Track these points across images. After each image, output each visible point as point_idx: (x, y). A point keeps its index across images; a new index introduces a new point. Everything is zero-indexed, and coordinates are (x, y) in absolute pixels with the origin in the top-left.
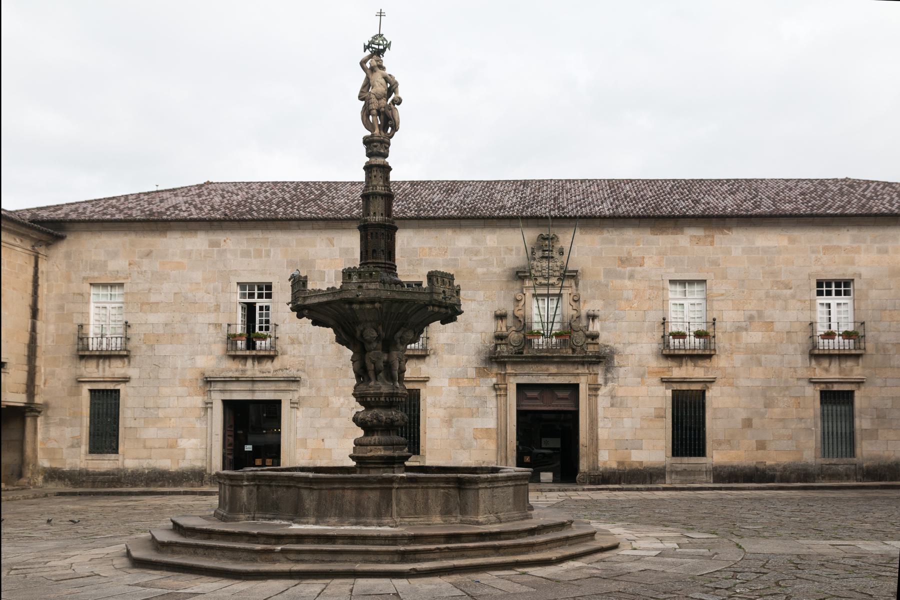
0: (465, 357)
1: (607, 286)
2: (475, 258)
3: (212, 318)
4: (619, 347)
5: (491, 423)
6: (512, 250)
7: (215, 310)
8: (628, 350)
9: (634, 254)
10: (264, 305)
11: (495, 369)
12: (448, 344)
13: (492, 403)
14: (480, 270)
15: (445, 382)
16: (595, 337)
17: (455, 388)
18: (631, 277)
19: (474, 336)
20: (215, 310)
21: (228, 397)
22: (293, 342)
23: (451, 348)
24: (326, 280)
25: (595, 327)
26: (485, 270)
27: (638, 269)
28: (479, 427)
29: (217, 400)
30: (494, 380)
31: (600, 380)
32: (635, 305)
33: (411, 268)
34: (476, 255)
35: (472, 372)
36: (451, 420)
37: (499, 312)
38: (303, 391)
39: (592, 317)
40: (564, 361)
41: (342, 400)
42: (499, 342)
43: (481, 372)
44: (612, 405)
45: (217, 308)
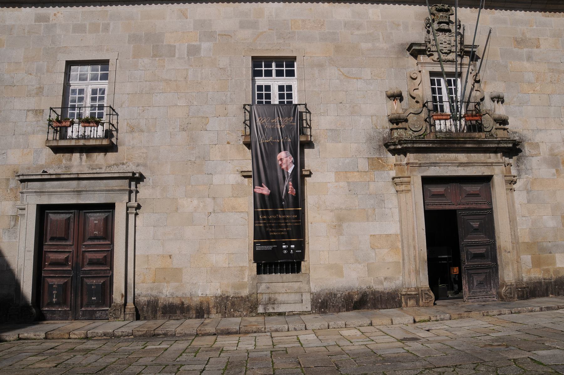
0: (354, 146)
1: (506, 67)
2: (357, 32)
3: (33, 103)
4: (527, 134)
5: (393, 228)
6: (399, 25)
7: (37, 94)
8: (538, 138)
9: (528, 35)
10: (99, 87)
11: (392, 159)
12: (331, 130)
13: (392, 202)
14: (364, 46)
15: (331, 177)
16: (503, 122)
17: (343, 184)
18: (529, 58)
19: (362, 120)
20: (37, 94)
21: (45, 200)
22: (132, 130)
23: (335, 134)
24: (177, 56)
25: (500, 110)
26: (370, 45)
27: (535, 50)
28: (377, 233)
29: (32, 202)
30: (393, 174)
31: (514, 172)
32: (538, 88)
33: (281, 41)
34: (358, 29)
35: (363, 164)
36: (340, 226)
37: (391, 92)
38: (144, 191)
39: (499, 99)
40: (480, 148)
41: (195, 202)
42: (395, 126)
43: (376, 165)
44: (529, 202)
45: (40, 91)
